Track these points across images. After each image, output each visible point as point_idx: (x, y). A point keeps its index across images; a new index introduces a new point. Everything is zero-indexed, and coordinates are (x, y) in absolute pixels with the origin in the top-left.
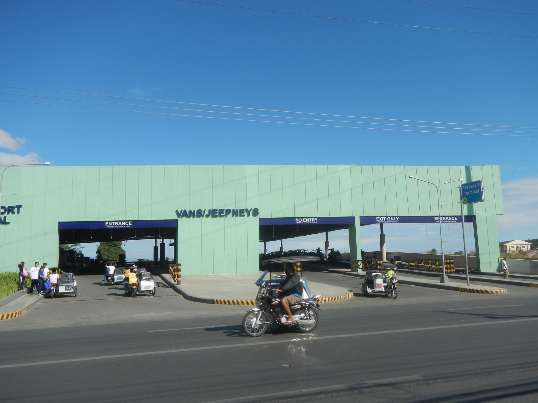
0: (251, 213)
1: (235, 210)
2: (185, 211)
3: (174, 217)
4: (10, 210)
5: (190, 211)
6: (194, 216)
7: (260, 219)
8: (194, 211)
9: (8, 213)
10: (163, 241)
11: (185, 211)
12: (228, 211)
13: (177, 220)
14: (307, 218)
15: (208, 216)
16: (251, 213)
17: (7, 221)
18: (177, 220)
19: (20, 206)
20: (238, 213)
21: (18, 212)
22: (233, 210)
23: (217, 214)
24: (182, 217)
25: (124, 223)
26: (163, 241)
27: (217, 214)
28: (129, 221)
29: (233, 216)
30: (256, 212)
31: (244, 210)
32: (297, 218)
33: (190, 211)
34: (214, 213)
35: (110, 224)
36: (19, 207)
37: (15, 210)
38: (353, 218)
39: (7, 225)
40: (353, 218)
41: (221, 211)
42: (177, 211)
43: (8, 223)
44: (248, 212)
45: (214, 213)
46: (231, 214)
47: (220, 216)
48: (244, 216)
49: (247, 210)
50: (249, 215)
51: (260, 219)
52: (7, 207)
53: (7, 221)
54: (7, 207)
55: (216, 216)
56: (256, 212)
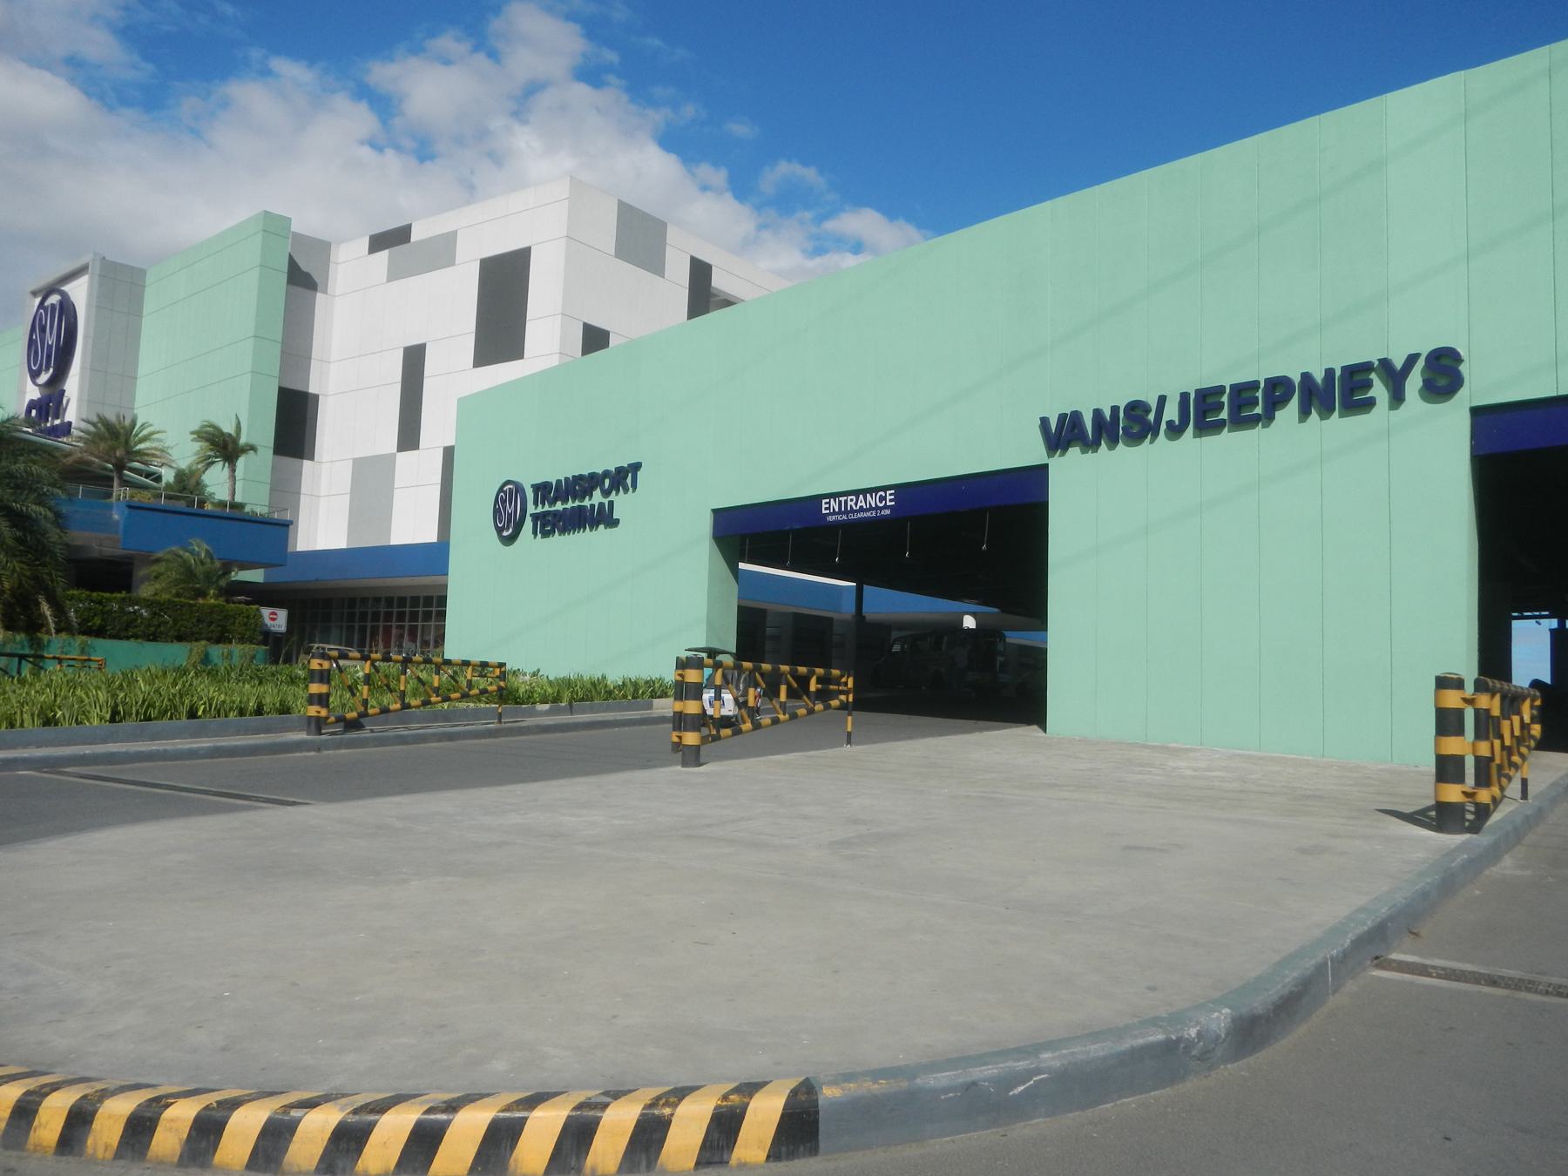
0: (1414, 382)
1: (1319, 376)
2: (1076, 416)
3: (1031, 452)
5: (1098, 414)
6: (1113, 442)
7: (1476, 412)
8: (1115, 409)
11: (1076, 416)
12: (1278, 391)
13: (1045, 467)
15: (1175, 431)
16: (1414, 382)
18: (1044, 468)
20: (1343, 391)
21: (634, 486)
22: (1306, 377)
23: (1224, 415)
24: (1065, 450)
25: (872, 500)
27: (1224, 415)
28: (885, 488)
29: (1304, 413)
30: (1443, 373)
31: (1366, 367)
33: (1098, 414)
34: (1209, 411)
36: (636, 467)
41: (1242, 394)
42: (1044, 422)
44: (1395, 378)
45: (1209, 411)
46: (1294, 402)
47: (1241, 421)
48: (1370, 404)
49: (1385, 364)
50: (1397, 398)
51: (1476, 412)
55: (1218, 426)
56: (1443, 373)
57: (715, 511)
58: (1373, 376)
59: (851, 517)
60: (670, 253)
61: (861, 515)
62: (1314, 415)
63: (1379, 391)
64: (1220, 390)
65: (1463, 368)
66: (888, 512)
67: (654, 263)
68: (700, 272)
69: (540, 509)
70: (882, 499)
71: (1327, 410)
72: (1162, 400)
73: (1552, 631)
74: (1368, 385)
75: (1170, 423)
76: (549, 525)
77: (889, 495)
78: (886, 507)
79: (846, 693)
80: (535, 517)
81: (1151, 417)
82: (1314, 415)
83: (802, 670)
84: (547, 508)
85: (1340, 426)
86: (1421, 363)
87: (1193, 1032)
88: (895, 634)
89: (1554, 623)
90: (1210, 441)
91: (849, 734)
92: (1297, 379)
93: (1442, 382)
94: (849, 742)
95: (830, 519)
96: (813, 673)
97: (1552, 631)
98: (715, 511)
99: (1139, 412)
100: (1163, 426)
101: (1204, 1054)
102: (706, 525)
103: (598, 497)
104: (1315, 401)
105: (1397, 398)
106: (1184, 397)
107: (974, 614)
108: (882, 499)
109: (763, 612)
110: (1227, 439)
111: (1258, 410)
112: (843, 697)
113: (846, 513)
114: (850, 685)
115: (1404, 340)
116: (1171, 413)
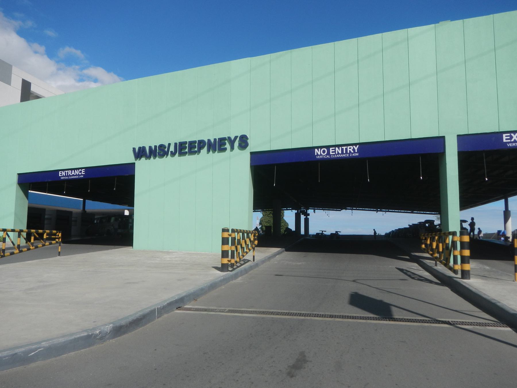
0: (236, 144)
1: (212, 141)
2: (144, 148)
3: (129, 158)
5: (150, 147)
7: (252, 153)
8: (155, 147)
11: (144, 148)
12: (201, 144)
13: (135, 163)
14: (338, 146)
15: (173, 154)
16: (236, 144)
18: (135, 163)
20: (218, 145)
22: (209, 140)
23: (187, 150)
24: (140, 158)
25: (77, 172)
27: (187, 150)
28: (82, 168)
29: (208, 151)
30: (244, 142)
31: (224, 139)
32: (318, 148)
33: (150, 147)
35: (64, 174)
38: (441, 140)
40: (441, 140)
41: (192, 144)
42: (134, 149)
46: (206, 148)
47: (191, 153)
48: (225, 149)
49: (229, 138)
50: (232, 148)
51: (252, 153)
55: (185, 154)
56: (244, 142)
57: (19, 174)
58: (226, 141)
59: (70, 178)
60: (13, 77)
61: (73, 177)
62: (211, 152)
63: (228, 146)
64: (185, 143)
65: (248, 141)
66: (82, 176)
68: (26, 86)
70: (81, 172)
71: (214, 151)
72: (169, 145)
74: (225, 144)
75: (171, 152)
77: (83, 171)
78: (82, 175)
79: (59, 239)
81: (166, 150)
82: (211, 152)
83: (40, 231)
85: (217, 156)
86: (238, 139)
87: (98, 332)
88: (96, 217)
89: (296, 211)
90: (182, 158)
91: (59, 252)
92: (207, 141)
93: (243, 144)
94: (59, 255)
95: (62, 178)
96: (45, 232)
99: (162, 148)
100: (170, 153)
101: (102, 337)
102: (15, 179)
104: (211, 148)
105: (232, 148)
106: (176, 144)
107: (128, 210)
108: (81, 172)
109: (43, 210)
110: (188, 158)
111: (196, 149)
112: (57, 240)
113: (68, 176)
114: (60, 235)
115: (234, 132)
116: (172, 149)
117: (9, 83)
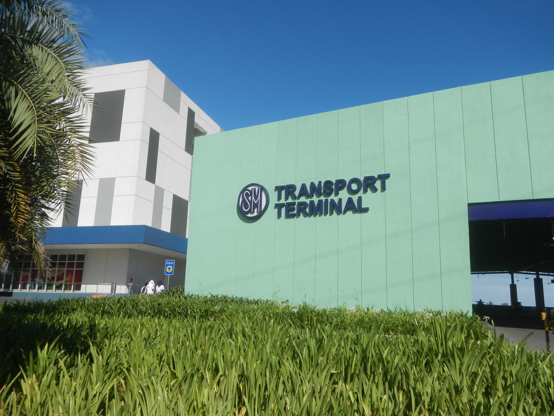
4: (369, 183)
9: (365, 191)
10: (538, 276)
17: (364, 206)
19: (387, 176)
21: (383, 188)
26: (538, 276)
36: (384, 177)
37: (378, 184)
39: (363, 215)
43: (366, 210)
52: (362, 179)
53: (364, 206)
54: (362, 179)
57: (469, 205)
60: (182, 103)
67: (176, 108)
68: (191, 114)
69: (283, 201)
73: (535, 279)
76: (289, 212)
80: (279, 207)
84: (290, 200)
97: (535, 279)
98: (469, 205)
102: (465, 210)
103: (344, 195)
117: (177, 110)
